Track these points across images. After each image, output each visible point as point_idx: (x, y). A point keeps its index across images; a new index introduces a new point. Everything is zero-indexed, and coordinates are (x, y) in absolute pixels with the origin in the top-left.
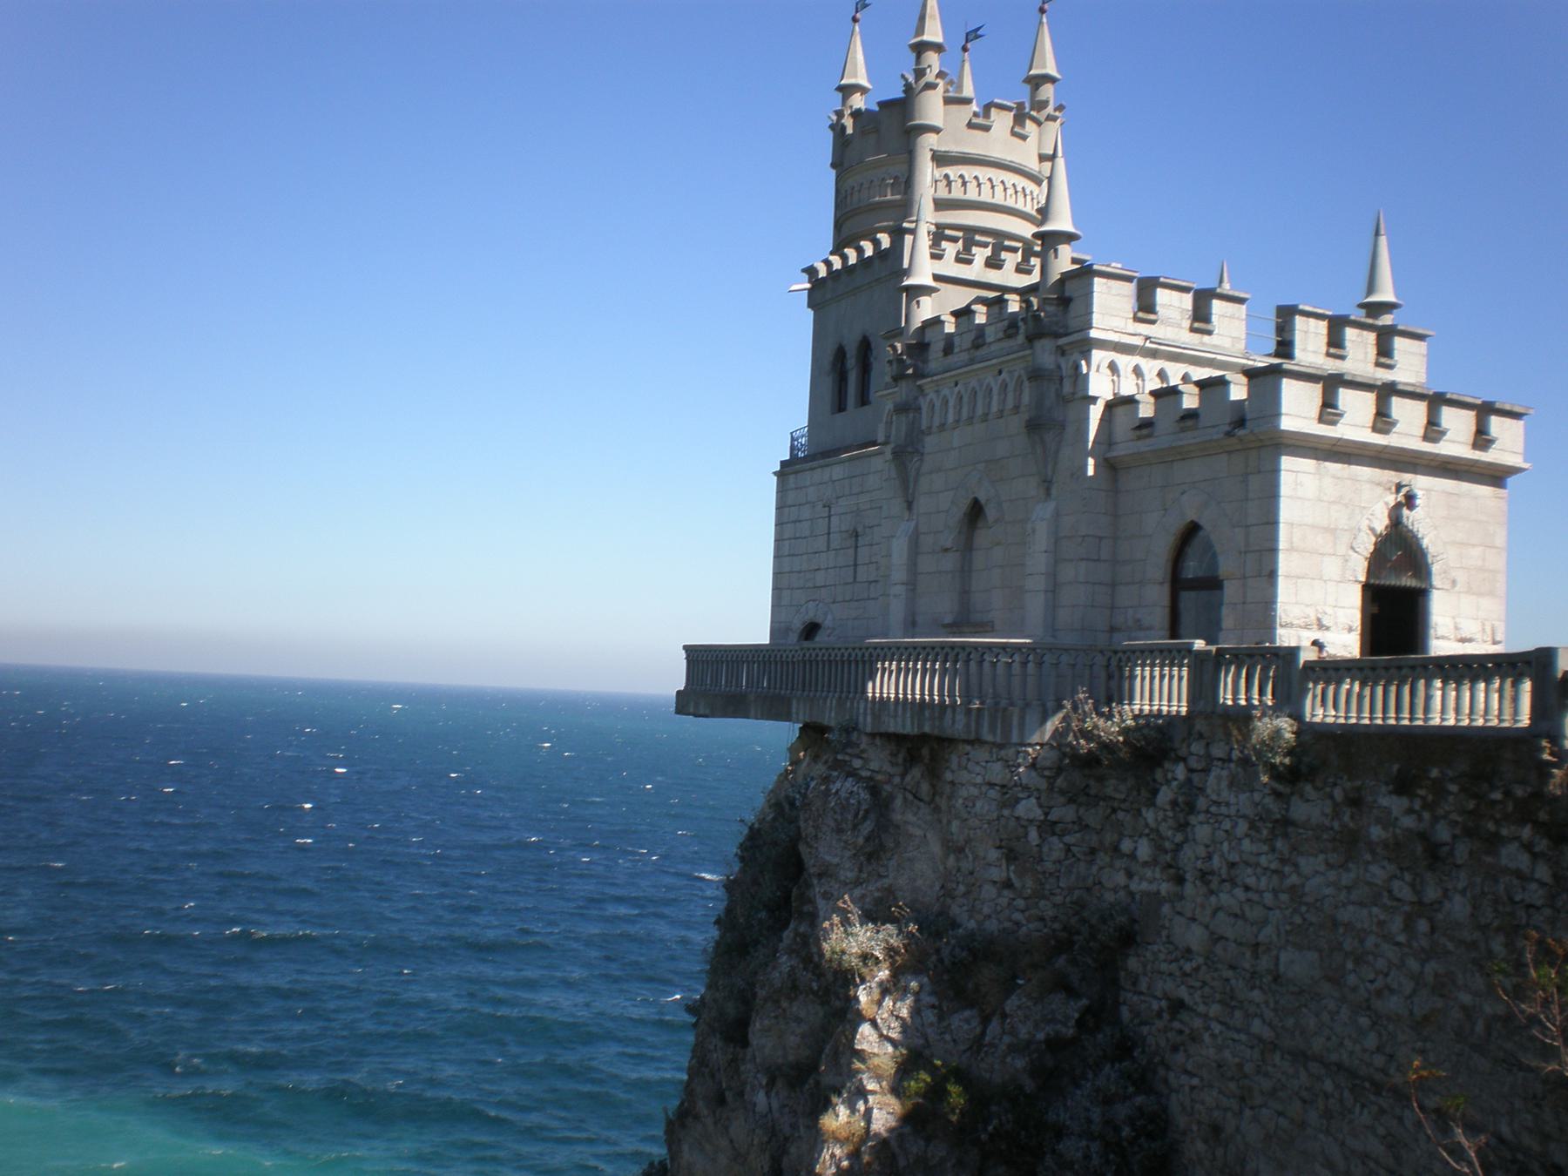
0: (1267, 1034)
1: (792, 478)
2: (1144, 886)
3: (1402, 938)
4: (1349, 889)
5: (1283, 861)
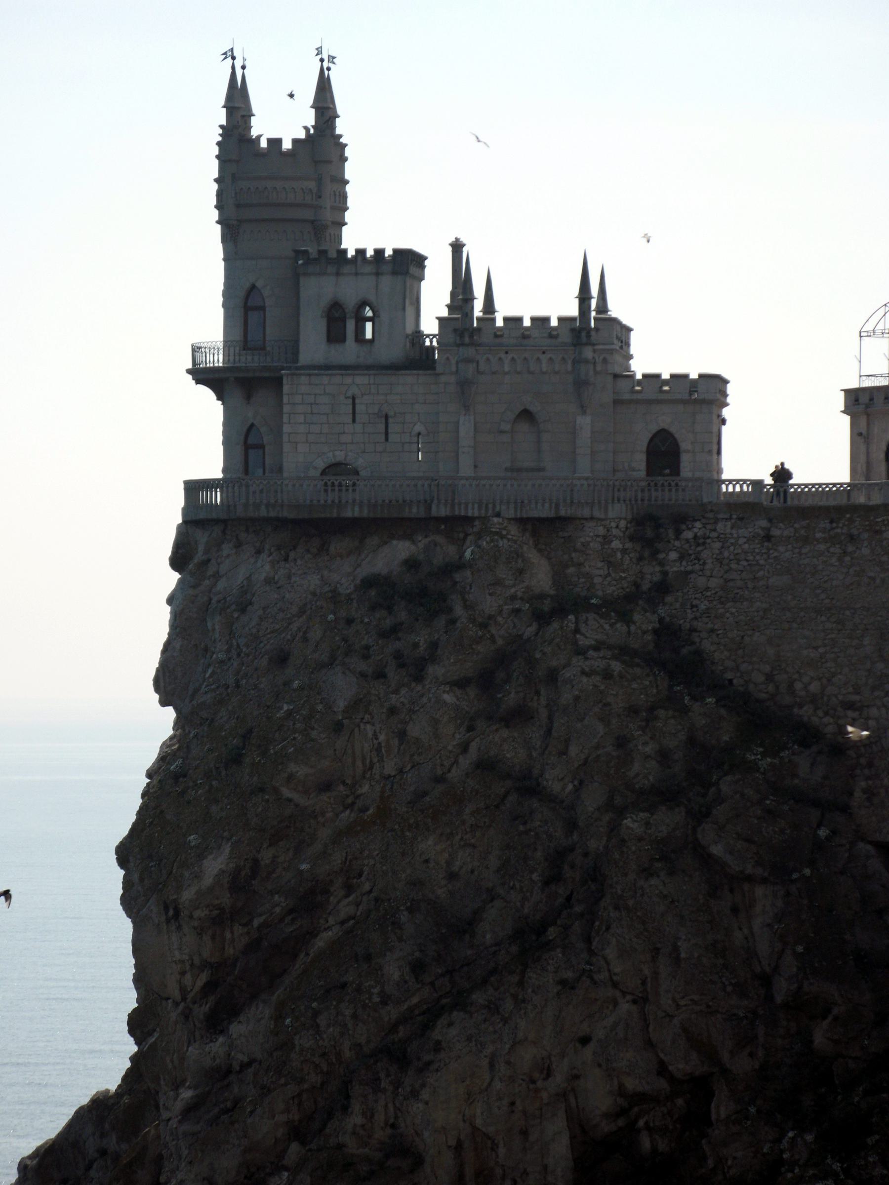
0: (765, 606)
1: (303, 378)
2: (675, 569)
3: (837, 564)
4: (806, 554)
5: (769, 549)
